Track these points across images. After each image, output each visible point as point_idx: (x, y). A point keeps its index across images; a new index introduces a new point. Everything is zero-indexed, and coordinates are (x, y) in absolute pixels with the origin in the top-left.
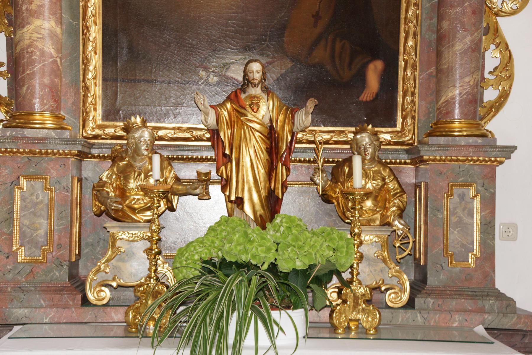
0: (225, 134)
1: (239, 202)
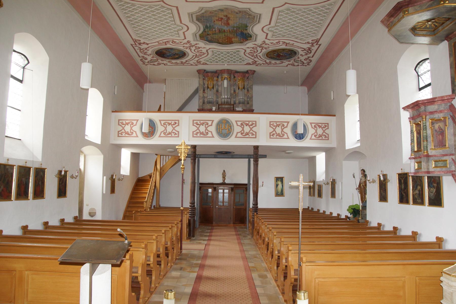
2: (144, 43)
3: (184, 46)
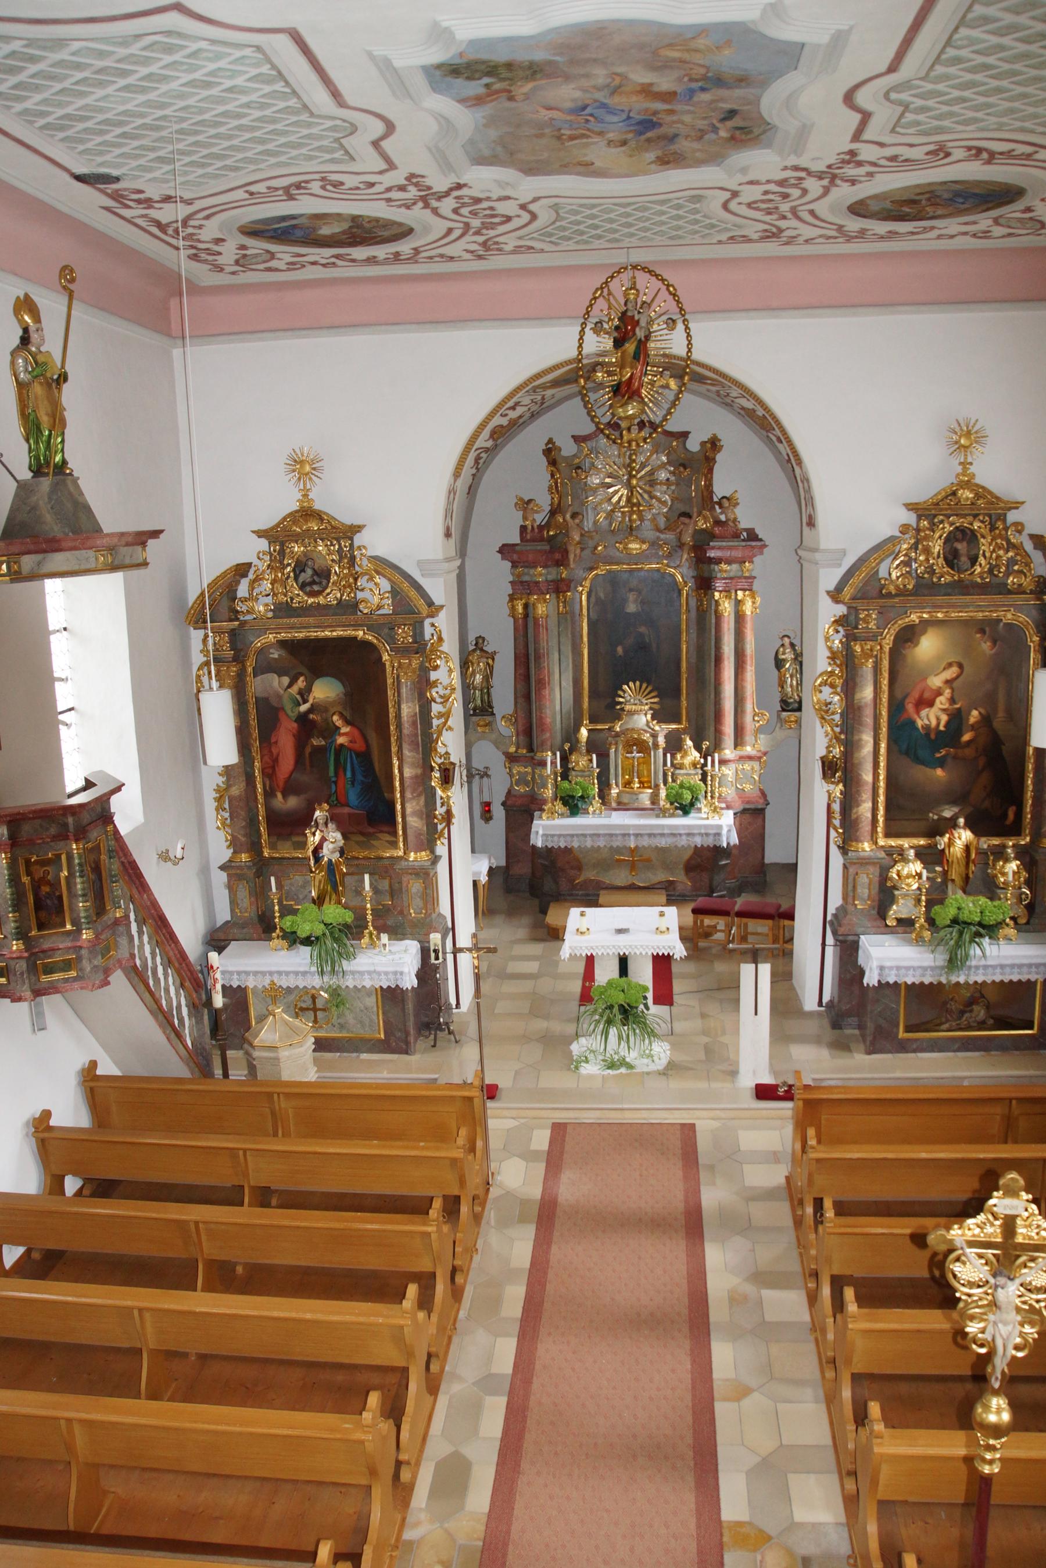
2: (167, 199)
3: (389, 200)
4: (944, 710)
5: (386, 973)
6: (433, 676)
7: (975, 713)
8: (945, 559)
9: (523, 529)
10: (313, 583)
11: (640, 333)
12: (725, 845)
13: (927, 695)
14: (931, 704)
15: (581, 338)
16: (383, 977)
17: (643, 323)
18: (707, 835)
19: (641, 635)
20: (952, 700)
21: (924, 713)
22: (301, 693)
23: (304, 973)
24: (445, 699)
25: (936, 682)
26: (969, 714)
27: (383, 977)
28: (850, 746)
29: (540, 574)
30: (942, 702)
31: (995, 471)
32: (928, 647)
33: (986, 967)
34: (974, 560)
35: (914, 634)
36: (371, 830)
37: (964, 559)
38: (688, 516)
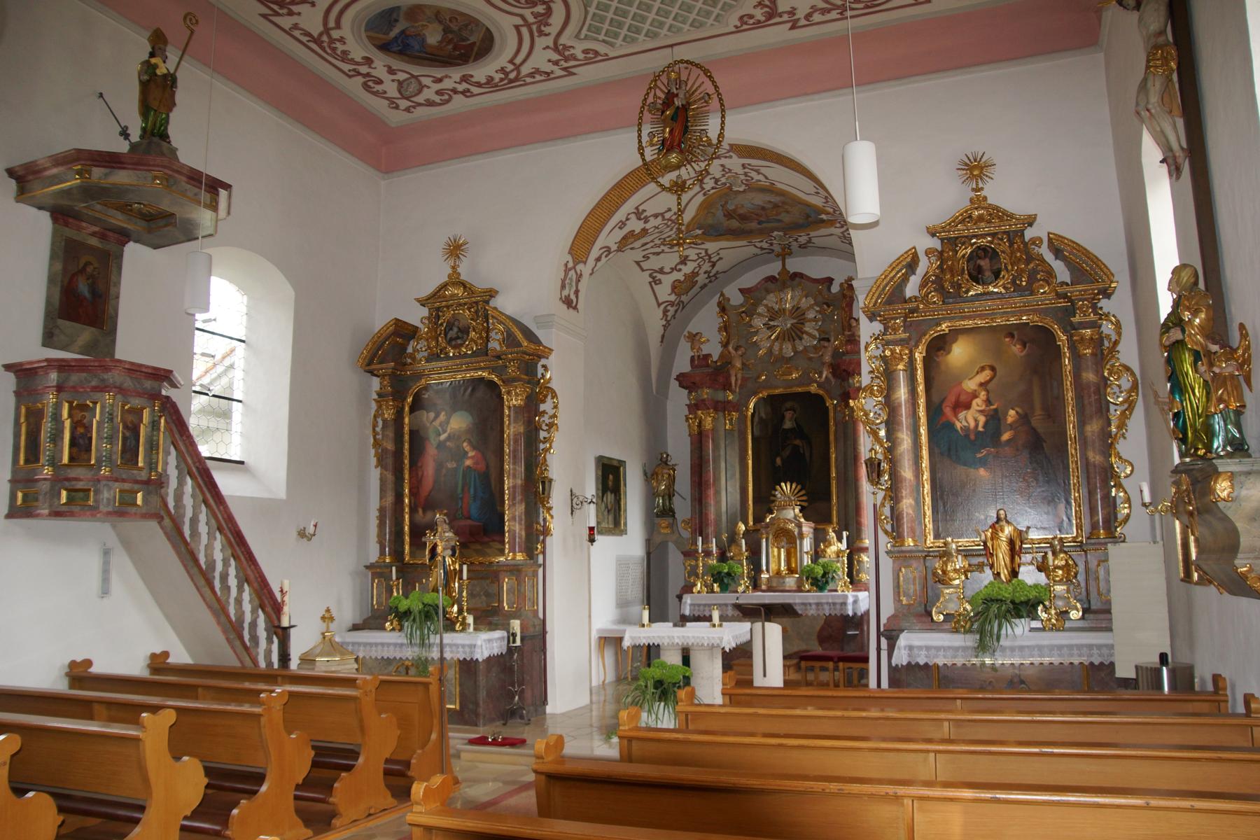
0: (989, 544)
1: (999, 574)
4: (981, 411)
5: (463, 646)
6: (542, 407)
7: (1012, 412)
8: (970, 275)
9: (692, 359)
10: (458, 338)
11: (678, 102)
12: (850, 613)
13: (963, 398)
14: (968, 406)
15: (641, 118)
16: (461, 649)
17: (681, 95)
18: (834, 604)
19: (796, 447)
20: (988, 402)
21: (962, 415)
22: (441, 425)
23: (402, 645)
24: (551, 425)
25: (971, 385)
26: (1006, 414)
27: (461, 649)
28: (891, 451)
29: (706, 393)
30: (978, 404)
31: (1006, 193)
32: (960, 353)
33: (1022, 648)
34: (997, 275)
35: (945, 343)
36: (486, 539)
37: (988, 274)
38: (828, 340)
